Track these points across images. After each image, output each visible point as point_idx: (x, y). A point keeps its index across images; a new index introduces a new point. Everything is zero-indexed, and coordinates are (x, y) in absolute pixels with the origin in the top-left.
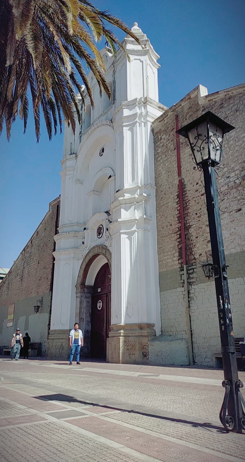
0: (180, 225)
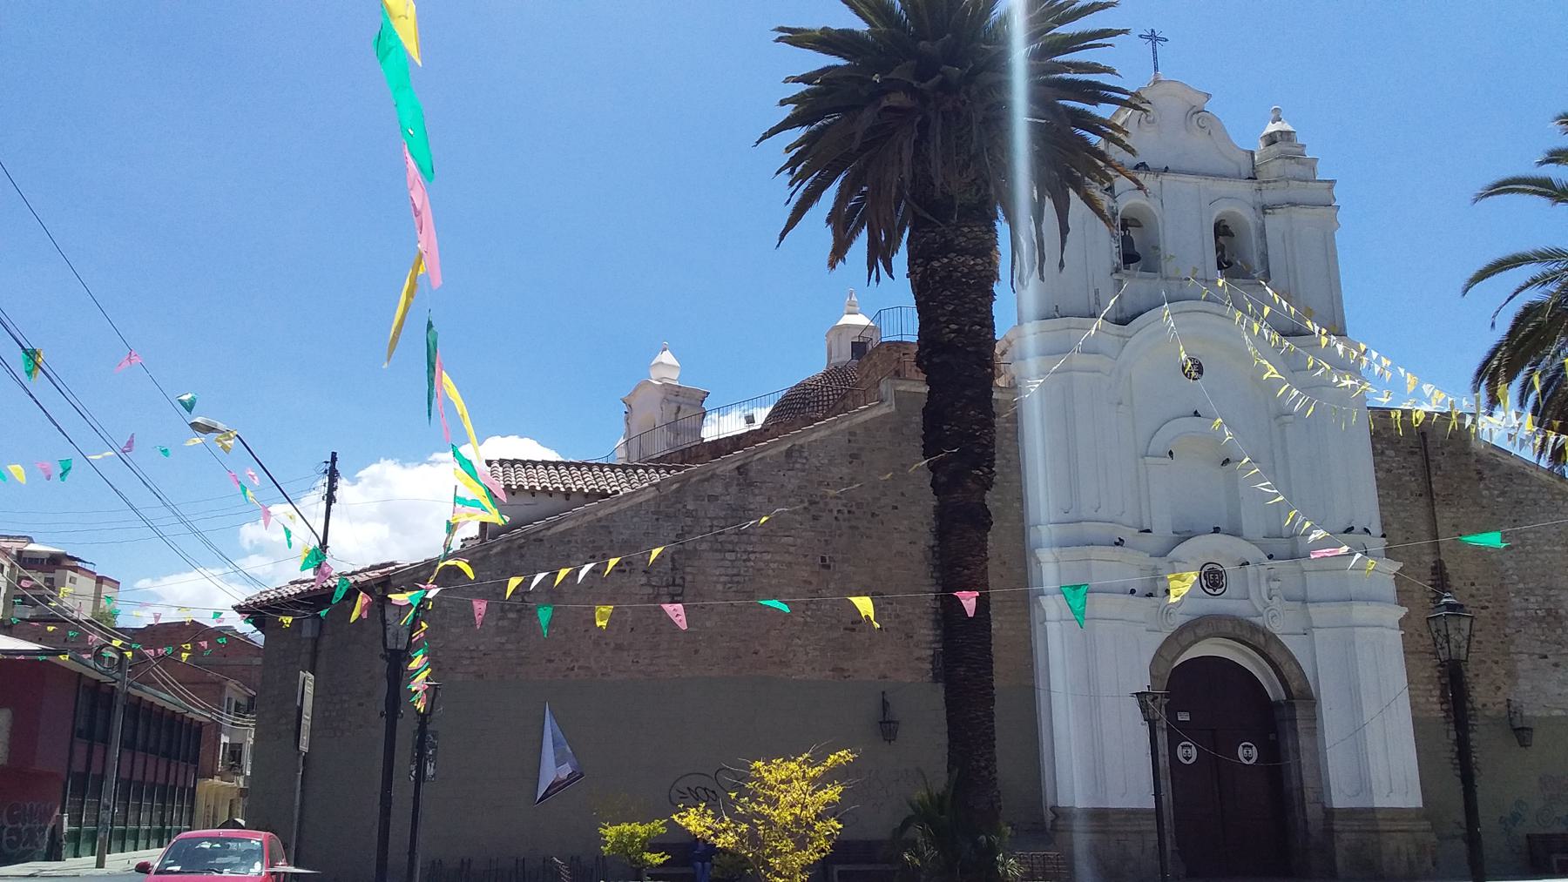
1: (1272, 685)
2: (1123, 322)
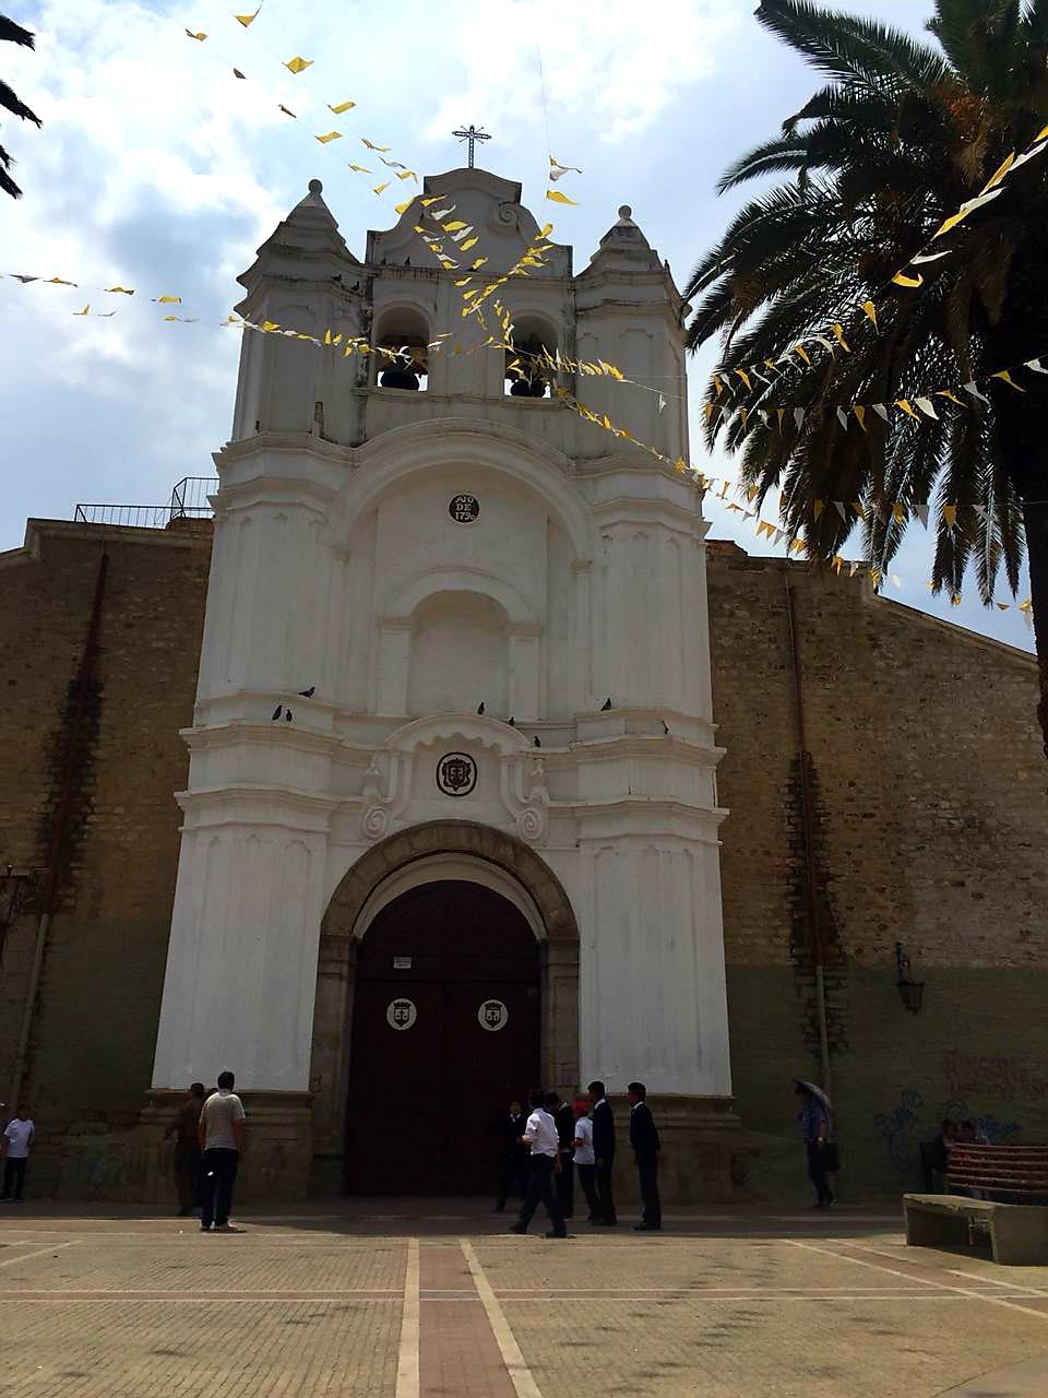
0: (799, 863)
2: (356, 445)
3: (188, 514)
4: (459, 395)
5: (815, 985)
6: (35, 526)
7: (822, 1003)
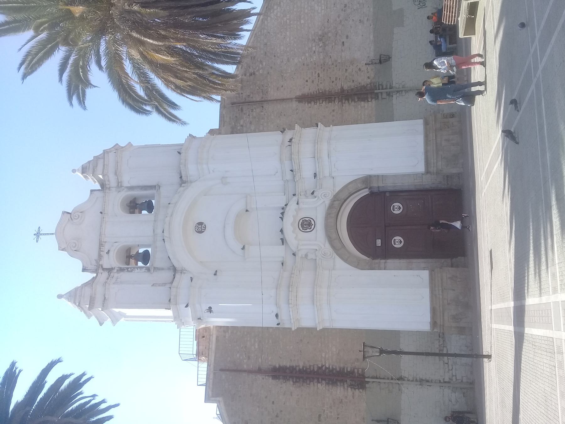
0: (337, 99)
1: (360, 194)
3: (195, 353)
4: (154, 231)
5: (382, 93)
6: (208, 399)
7: (388, 90)
